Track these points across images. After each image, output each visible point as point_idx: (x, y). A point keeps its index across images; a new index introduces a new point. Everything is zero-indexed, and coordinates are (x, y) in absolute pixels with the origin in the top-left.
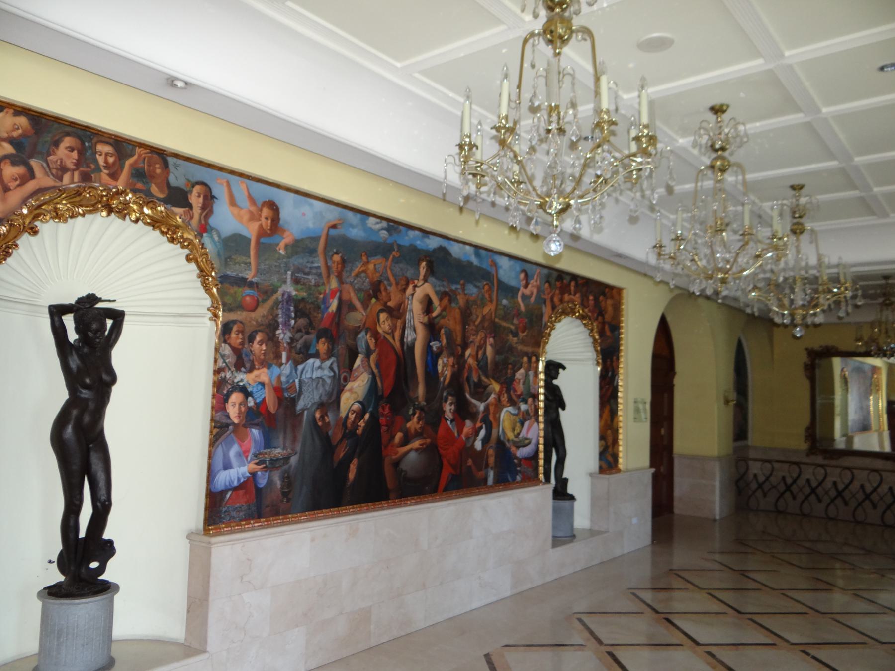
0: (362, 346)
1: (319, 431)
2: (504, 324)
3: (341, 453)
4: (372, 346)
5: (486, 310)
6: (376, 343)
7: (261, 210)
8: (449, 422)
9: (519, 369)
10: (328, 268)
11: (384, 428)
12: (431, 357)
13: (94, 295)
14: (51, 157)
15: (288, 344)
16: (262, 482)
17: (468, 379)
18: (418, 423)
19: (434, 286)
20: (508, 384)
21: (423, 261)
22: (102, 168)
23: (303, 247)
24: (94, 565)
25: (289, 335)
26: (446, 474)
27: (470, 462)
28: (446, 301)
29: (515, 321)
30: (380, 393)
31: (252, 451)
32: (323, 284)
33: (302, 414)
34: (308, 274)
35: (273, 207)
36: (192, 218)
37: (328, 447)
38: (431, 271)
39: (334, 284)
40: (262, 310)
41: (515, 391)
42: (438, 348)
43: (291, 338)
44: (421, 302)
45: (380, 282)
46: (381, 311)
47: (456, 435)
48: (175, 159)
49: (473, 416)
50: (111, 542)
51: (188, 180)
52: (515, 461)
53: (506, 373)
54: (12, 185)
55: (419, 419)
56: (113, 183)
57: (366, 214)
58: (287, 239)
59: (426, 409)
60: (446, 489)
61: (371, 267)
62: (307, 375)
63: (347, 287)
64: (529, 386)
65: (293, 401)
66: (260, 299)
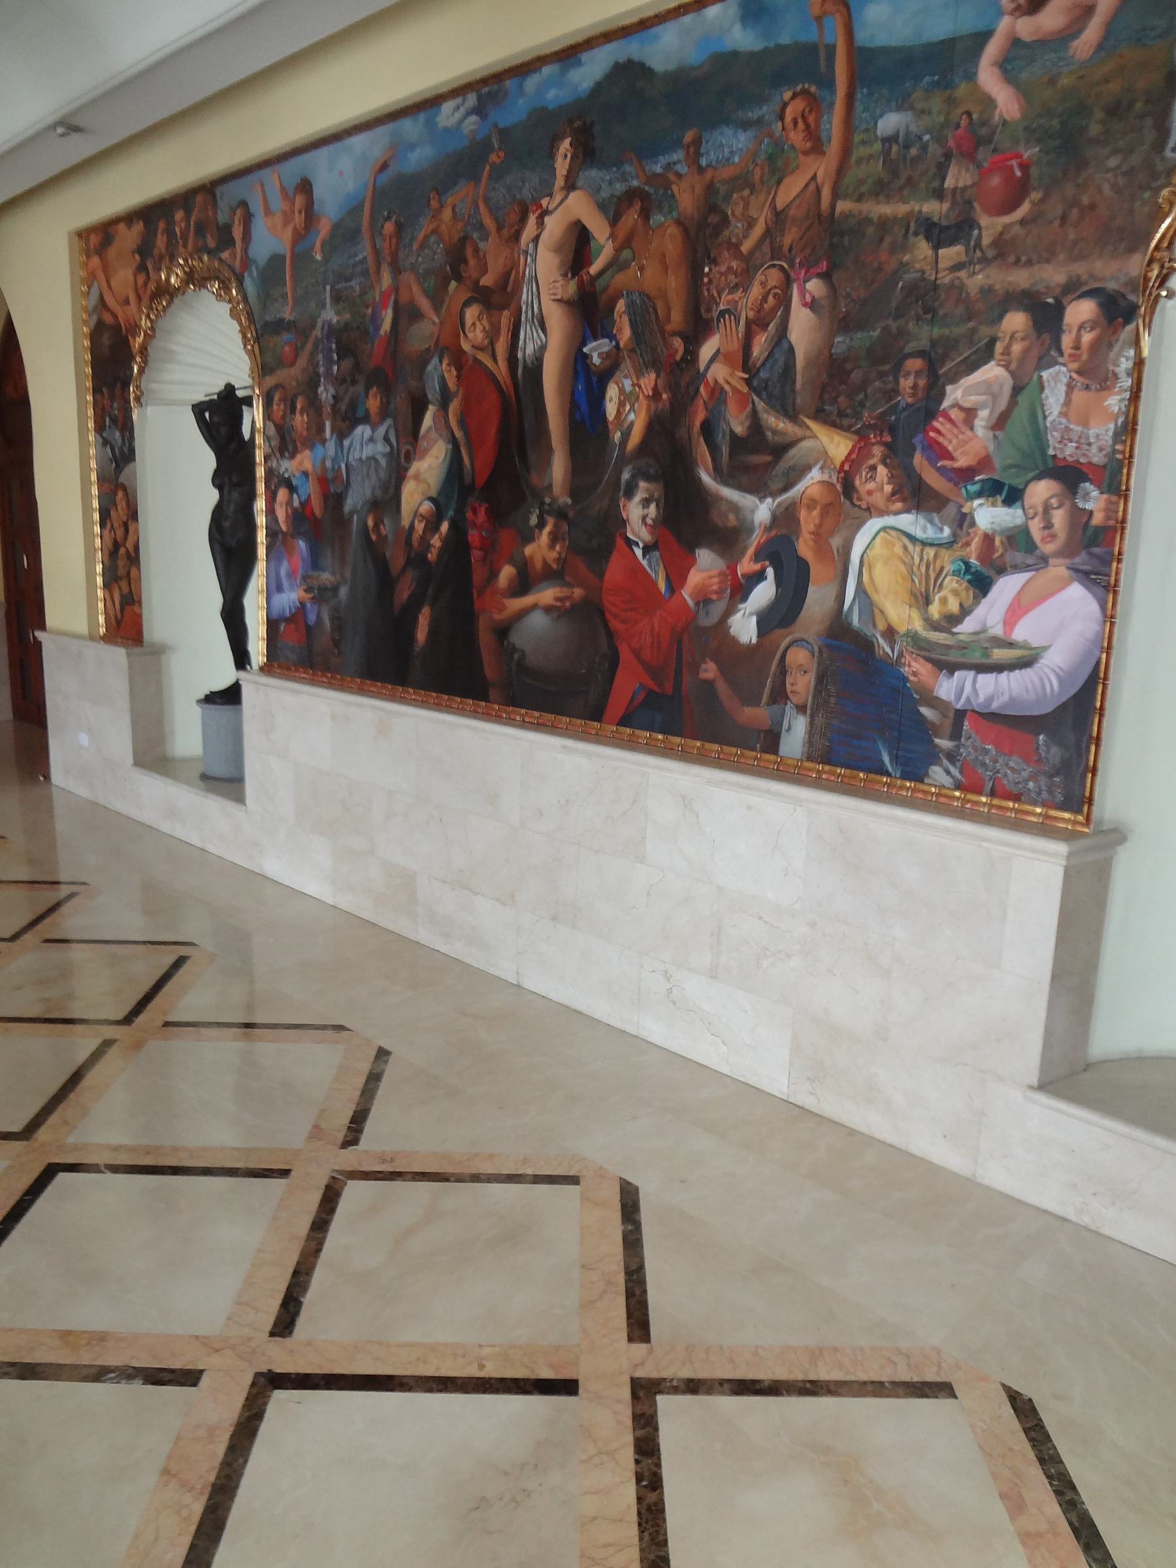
0: (433, 391)
1: (373, 550)
2: (886, 209)
3: (403, 592)
4: (452, 384)
5: (790, 190)
6: (458, 376)
7: (293, 203)
8: (639, 552)
9: (972, 366)
10: (376, 252)
11: (476, 554)
12: (588, 383)
15: (333, 407)
16: (312, 618)
17: (708, 430)
18: (552, 547)
21: (563, 138)
23: (345, 233)
25: (332, 391)
26: (627, 685)
27: (709, 670)
28: (631, 217)
29: (957, 177)
30: (468, 480)
31: (300, 571)
32: (372, 287)
33: (350, 520)
34: (348, 280)
35: (305, 187)
37: (385, 582)
38: (586, 154)
39: (386, 280)
40: (302, 361)
41: (938, 452)
42: (605, 356)
43: (334, 397)
44: (558, 249)
45: (464, 239)
46: (467, 304)
49: (728, 540)
52: (924, 710)
53: (895, 391)
55: (554, 538)
57: (428, 104)
58: (324, 229)
59: (571, 514)
60: (624, 721)
61: (447, 214)
62: (355, 455)
63: (408, 278)
64: (1039, 436)
65: (340, 498)
66: (299, 345)
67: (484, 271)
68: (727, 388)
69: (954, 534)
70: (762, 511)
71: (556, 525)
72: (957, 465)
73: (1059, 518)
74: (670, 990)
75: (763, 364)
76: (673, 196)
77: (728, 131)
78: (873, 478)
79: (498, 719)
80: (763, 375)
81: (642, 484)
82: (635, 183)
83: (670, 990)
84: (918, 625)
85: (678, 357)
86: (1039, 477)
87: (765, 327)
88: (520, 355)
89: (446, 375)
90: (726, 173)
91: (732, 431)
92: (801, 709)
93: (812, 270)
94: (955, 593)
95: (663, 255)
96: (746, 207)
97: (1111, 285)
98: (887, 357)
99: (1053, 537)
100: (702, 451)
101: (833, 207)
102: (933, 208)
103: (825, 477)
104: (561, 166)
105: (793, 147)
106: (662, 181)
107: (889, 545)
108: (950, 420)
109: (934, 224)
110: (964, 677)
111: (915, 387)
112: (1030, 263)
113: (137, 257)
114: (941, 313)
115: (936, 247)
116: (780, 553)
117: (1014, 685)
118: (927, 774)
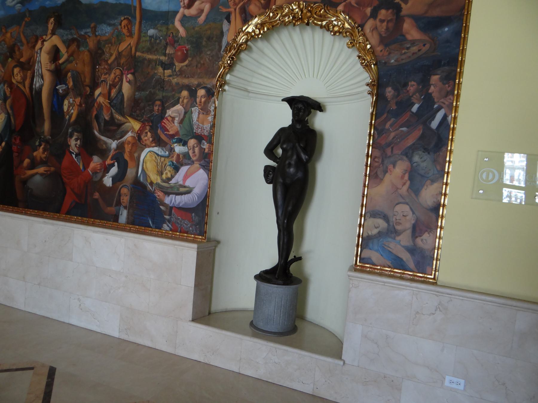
4: (8, 94)
5: (123, 47)
6: (11, 91)
8: (74, 156)
9: (174, 105)
11: (15, 154)
12: (57, 99)
17: (97, 117)
18: (43, 153)
19: (61, 37)
20: (155, 123)
26: (69, 201)
27: (97, 195)
28: (73, 47)
29: (169, 50)
38: (59, 24)
44: (48, 53)
45: (15, 45)
46: (15, 66)
47: (81, 167)
49: (103, 153)
52: (161, 207)
53: (153, 110)
55: (44, 150)
60: (68, 213)
61: (8, 35)
67: (22, 56)
68: (103, 105)
69: (169, 154)
70: (114, 144)
71: (45, 146)
72: (170, 133)
73: (197, 150)
74: (80, 305)
75: (115, 98)
76: (87, 42)
77: (105, 26)
78: (146, 136)
79: (21, 213)
80: (114, 102)
81: (76, 134)
82: (75, 36)
83: (80, 305)
84: (159, 181)
85: (88, 93)
86: (191, 138)
87: (115, 87)
88: (34, 87)
89: (6, 90)
90: (104, 38)
91: (105, 119)
92: (125, 208)
93: (130, 71)
94: (170, 171)
95: (84, 61)
96: (110, 49)
97: (209, 86)
98: (150, 100)
99: (195, 155)
100: (95, 124)
101: (135, 53)
102: (163, 58)
103: (133, 135)
104: (51, 27)
105: (124, 34)
106: (84, 37)
107: (151, 156)
108: (168, 121)
109: (164, 63)
110: (172, 197)
111: (158, 109)
112: (188, 77)
114: (165, 89)
115: (164, 69)
116: (119, 157)
117: (186, 199)
118: (162, 227)
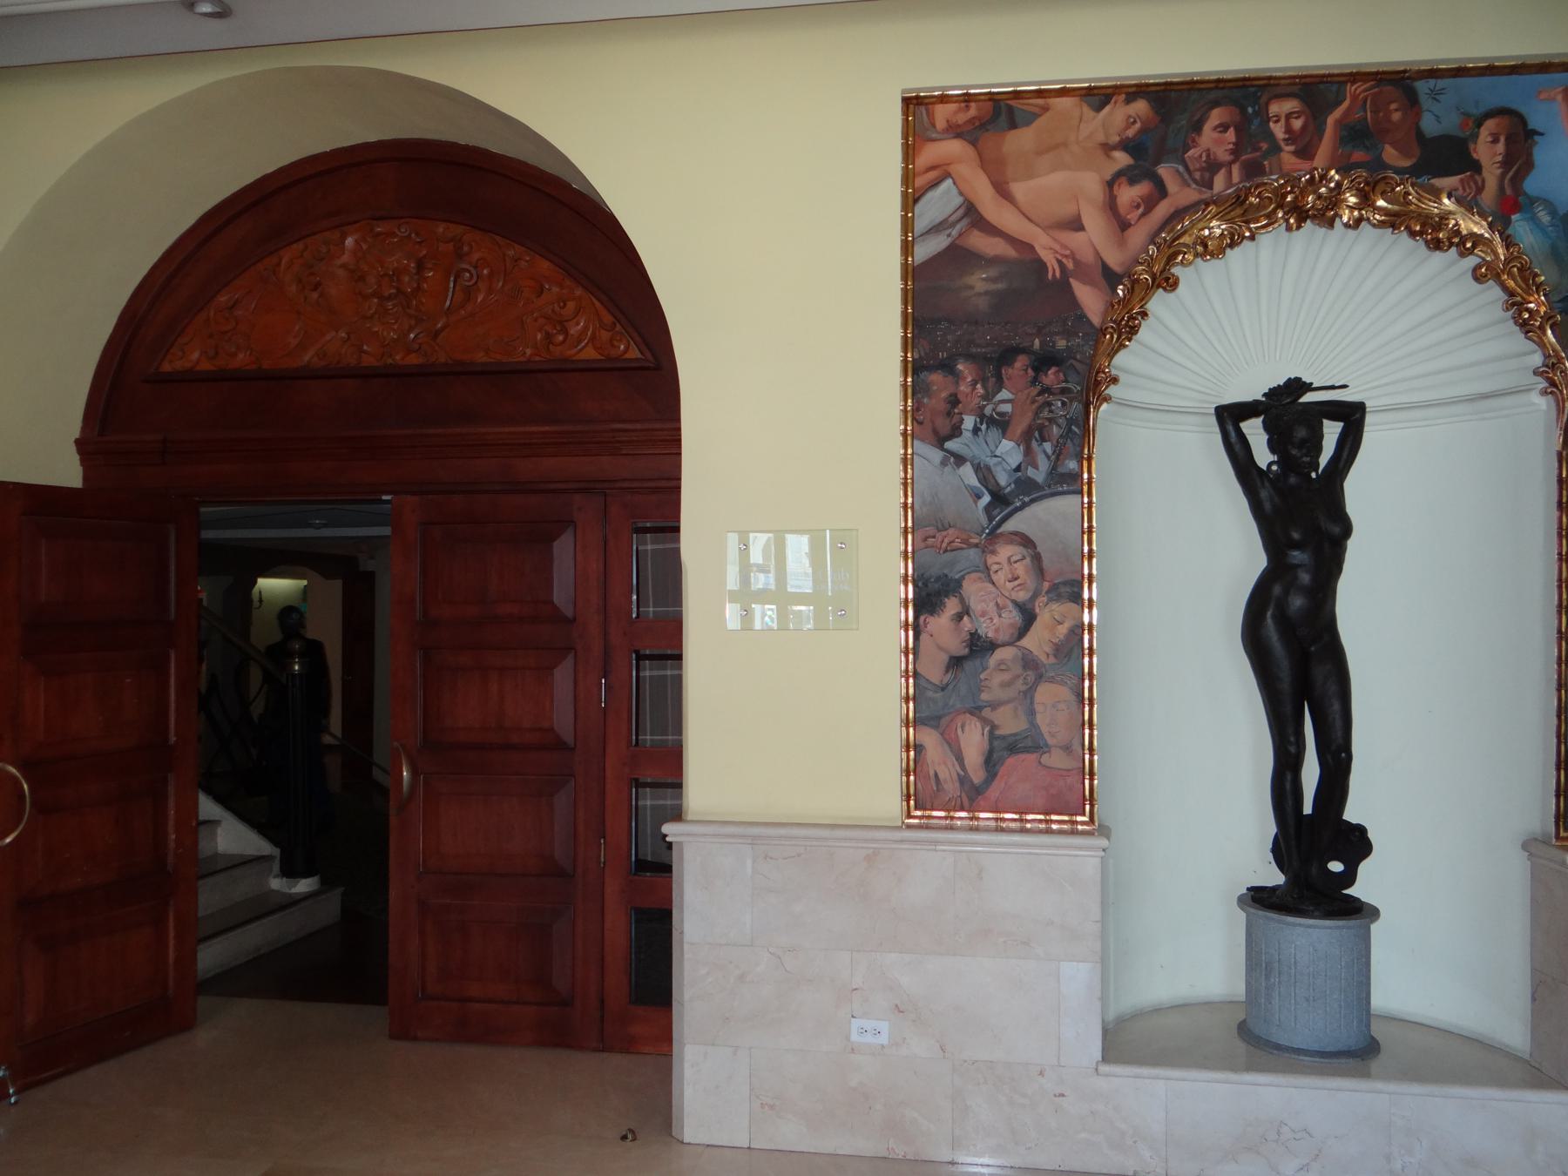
13: (1298, 380)
14: (1190, 153)
22: (1282, 144)
24: (1336, 867)
36: (1480, 190)
48: (1432, 82)
50: (1361, 830)
51: (1467, 115)
54: (1132, 216)
56: (1306, 165)
113: (1122, 159)
